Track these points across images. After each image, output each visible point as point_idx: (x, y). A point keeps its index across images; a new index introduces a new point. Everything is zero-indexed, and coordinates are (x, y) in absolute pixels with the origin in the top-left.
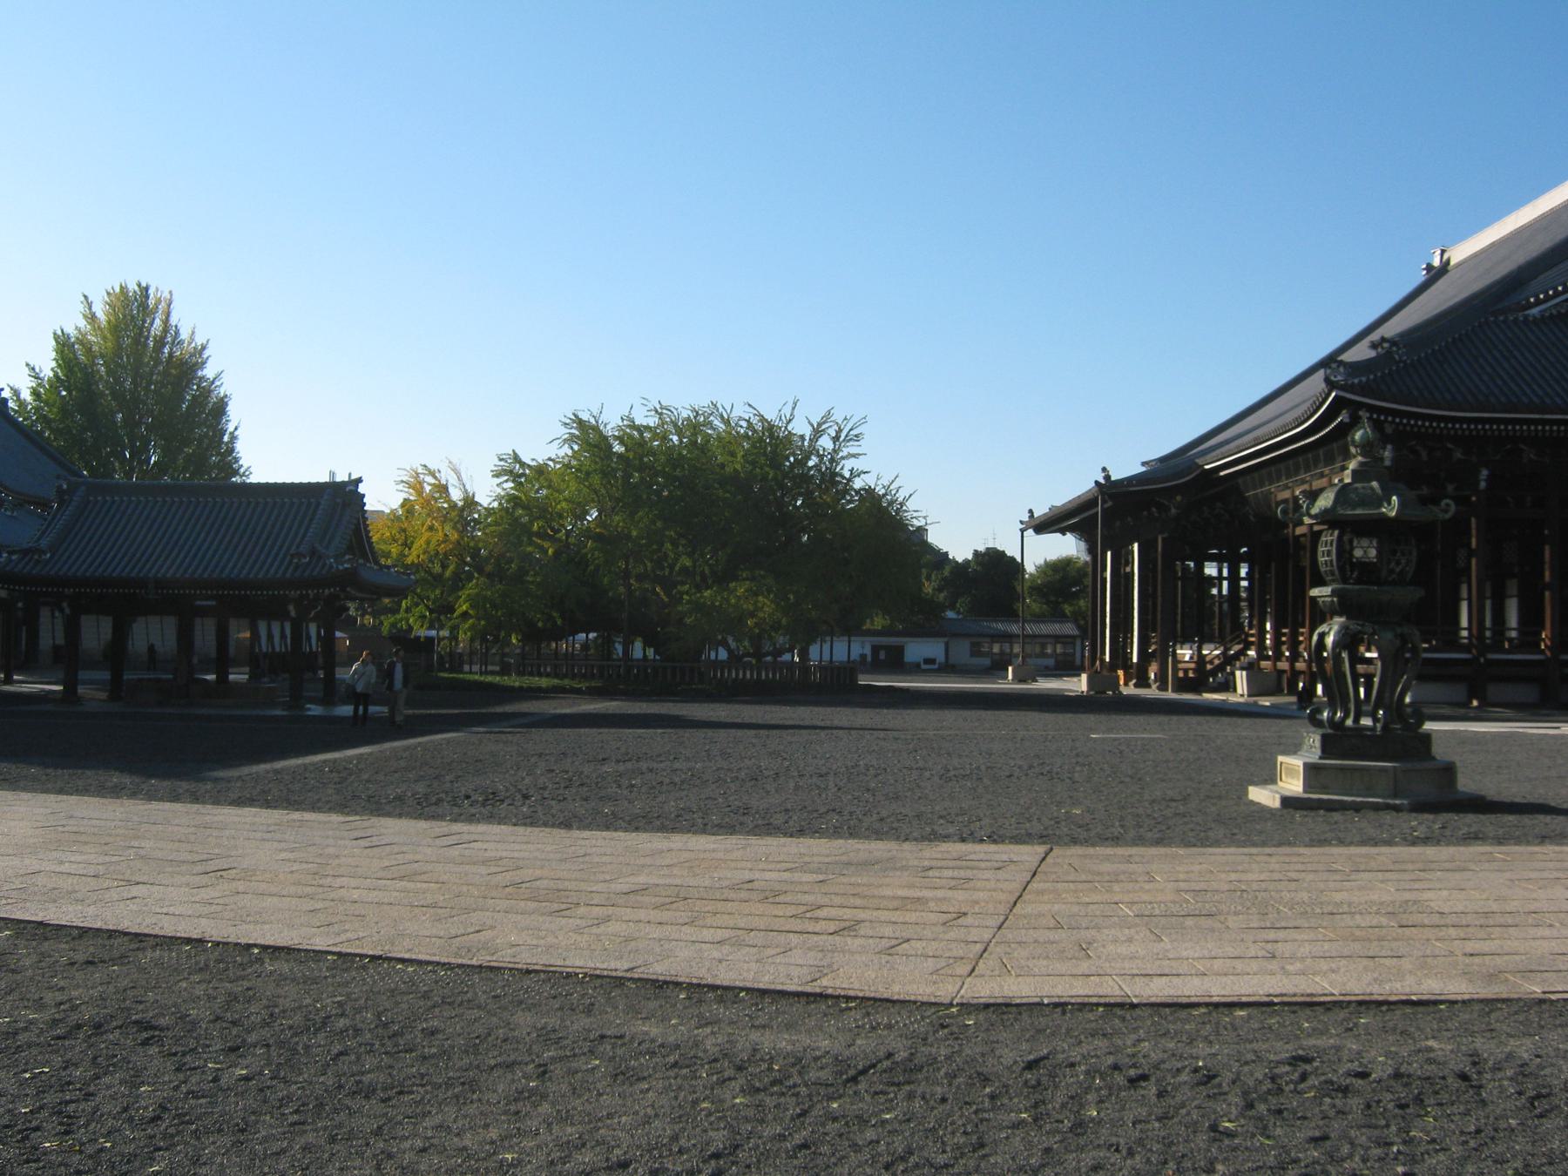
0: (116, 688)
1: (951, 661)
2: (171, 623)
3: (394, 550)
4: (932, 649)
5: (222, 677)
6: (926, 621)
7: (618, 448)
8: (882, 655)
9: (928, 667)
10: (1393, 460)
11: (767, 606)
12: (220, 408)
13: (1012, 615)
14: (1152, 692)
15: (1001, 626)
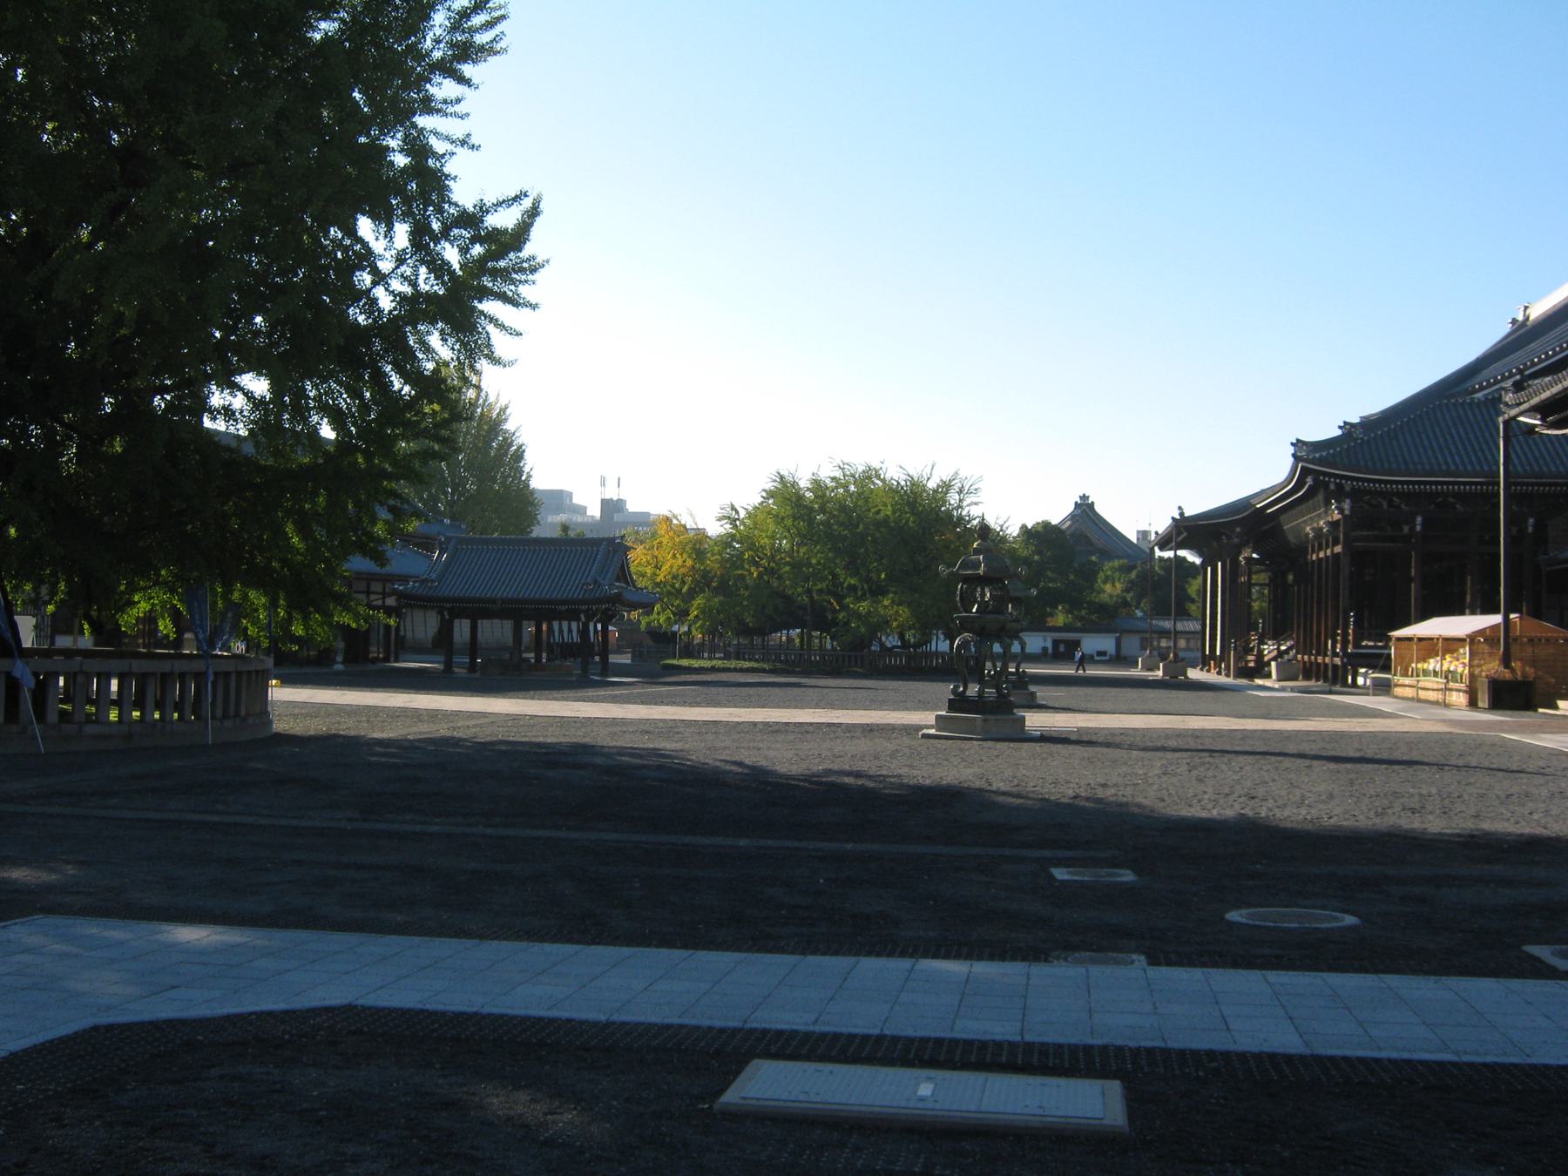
0: (472, 667)
1: (1124, 652)
2: (508, 625)
3: (649, 571)
4: (1106, 643)
5: (538, 658)
6: (1104, 618)
7: (808, 494)
8: (1062, 648)
9: (1101, 658)
10: (1352, 509)
11: (904, 613)
12: (519, 455)
13: (1183, 613)
14: (1223, 679)
15: (1167, 624)
